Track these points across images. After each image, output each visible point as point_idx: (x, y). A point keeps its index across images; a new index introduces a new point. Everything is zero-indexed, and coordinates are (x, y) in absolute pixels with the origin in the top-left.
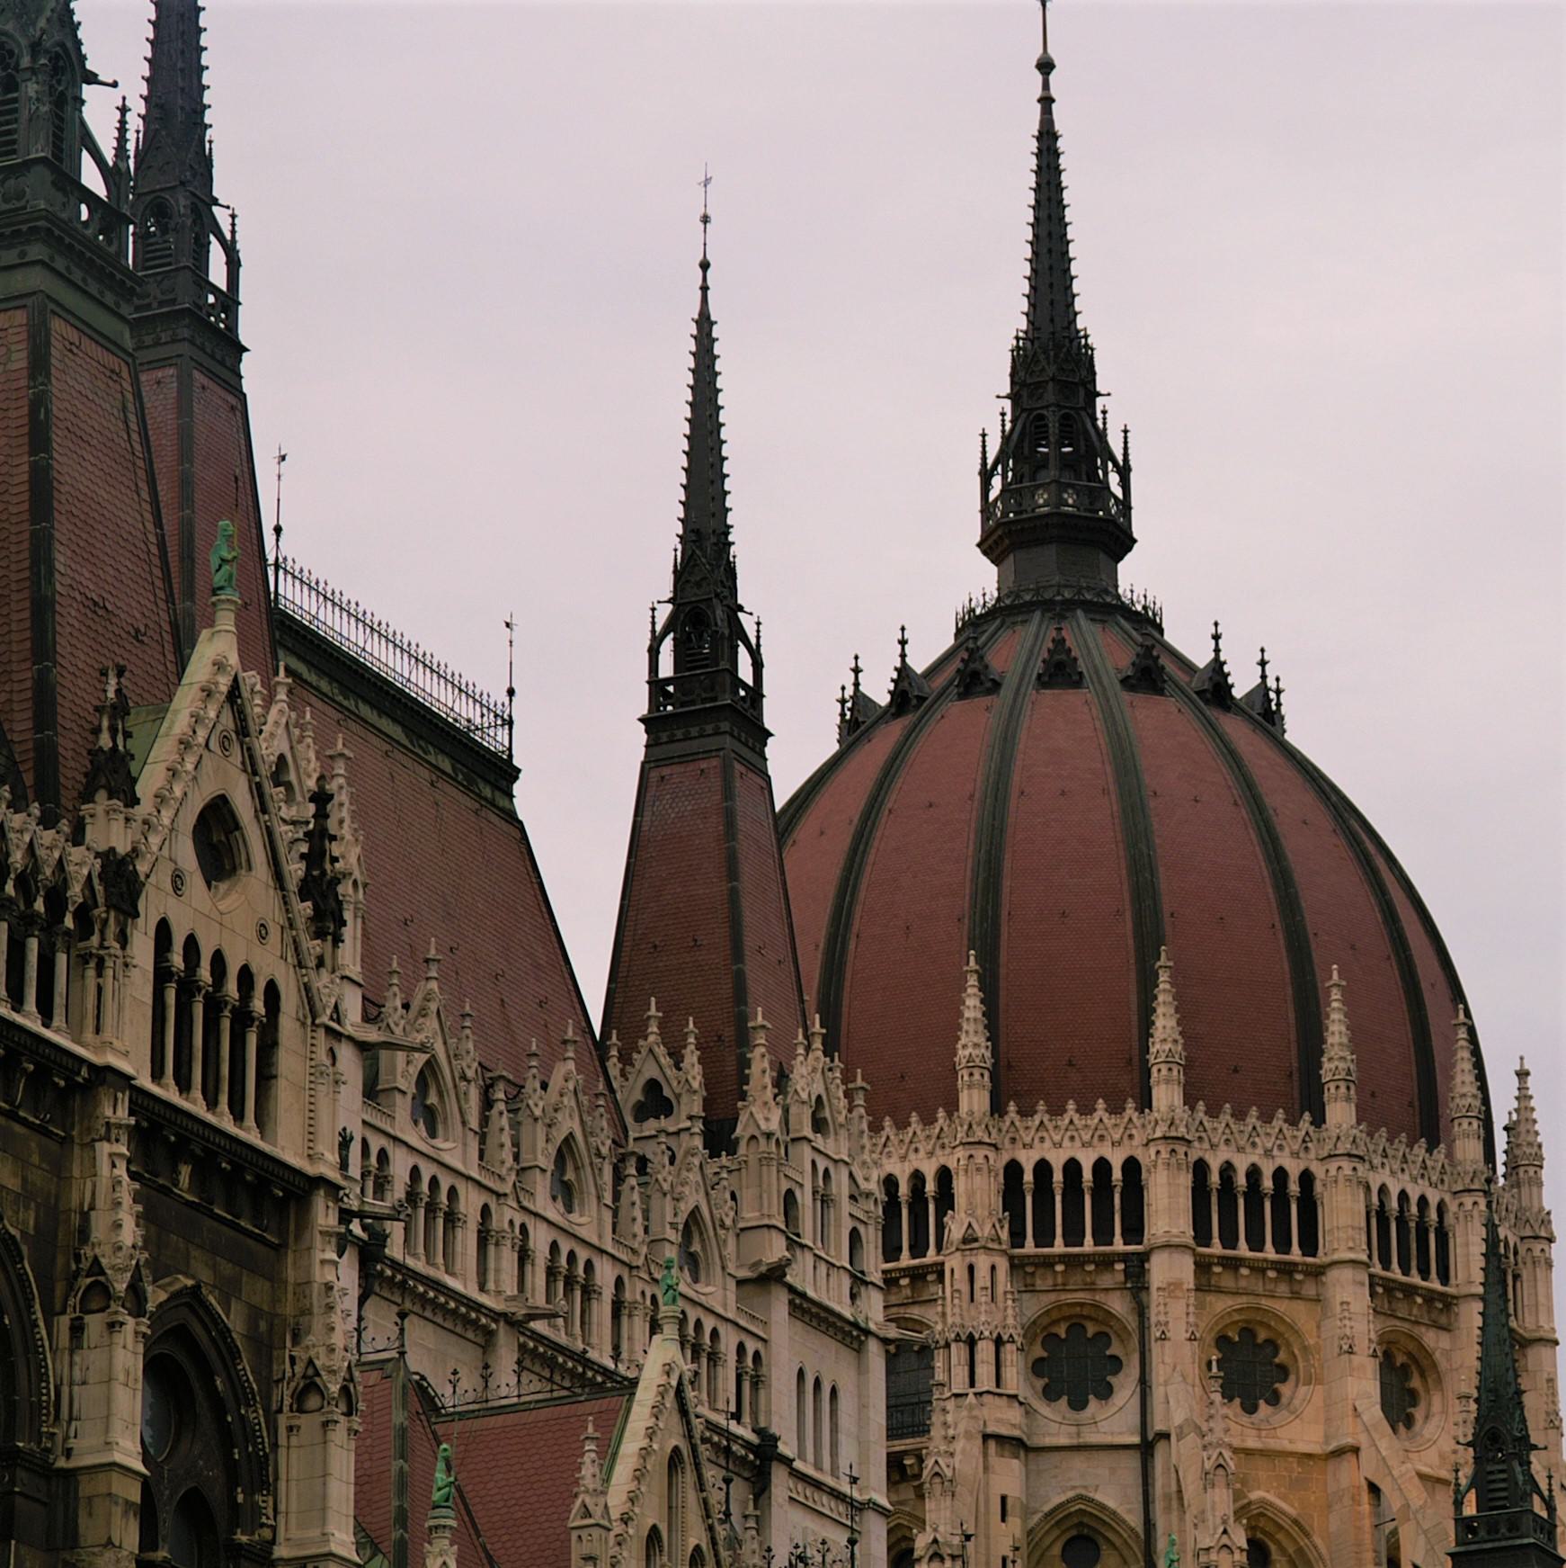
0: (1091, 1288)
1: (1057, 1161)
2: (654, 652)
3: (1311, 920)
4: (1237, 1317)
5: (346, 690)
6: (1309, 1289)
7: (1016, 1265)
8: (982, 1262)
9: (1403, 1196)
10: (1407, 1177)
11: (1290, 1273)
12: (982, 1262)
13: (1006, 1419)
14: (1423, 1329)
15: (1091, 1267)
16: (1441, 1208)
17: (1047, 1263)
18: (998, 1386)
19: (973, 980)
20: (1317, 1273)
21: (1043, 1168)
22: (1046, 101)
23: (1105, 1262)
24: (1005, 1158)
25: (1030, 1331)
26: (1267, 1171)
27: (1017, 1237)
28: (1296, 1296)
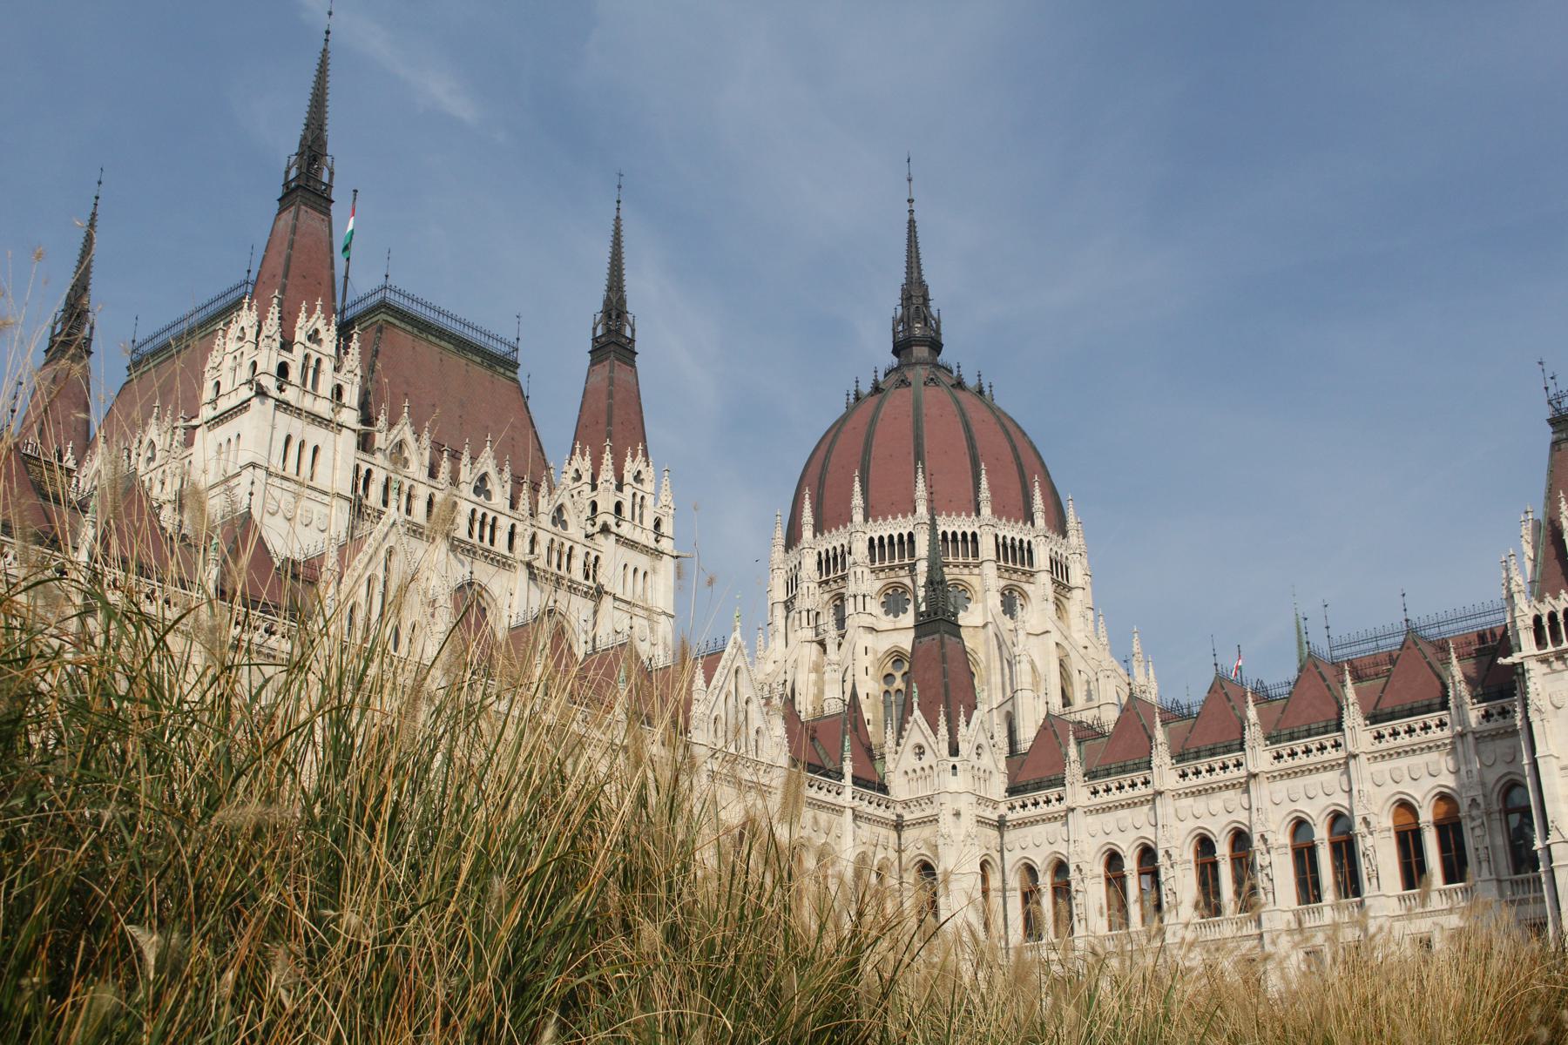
2: (595, 329)
3: (979, 452)
5: (421, 331)
6: (976, 571)
8: (859, 570)
12: (859, 570)
13: (867, 621)
22: (911, 212)
25: (879, 593)
27: (873, 561)
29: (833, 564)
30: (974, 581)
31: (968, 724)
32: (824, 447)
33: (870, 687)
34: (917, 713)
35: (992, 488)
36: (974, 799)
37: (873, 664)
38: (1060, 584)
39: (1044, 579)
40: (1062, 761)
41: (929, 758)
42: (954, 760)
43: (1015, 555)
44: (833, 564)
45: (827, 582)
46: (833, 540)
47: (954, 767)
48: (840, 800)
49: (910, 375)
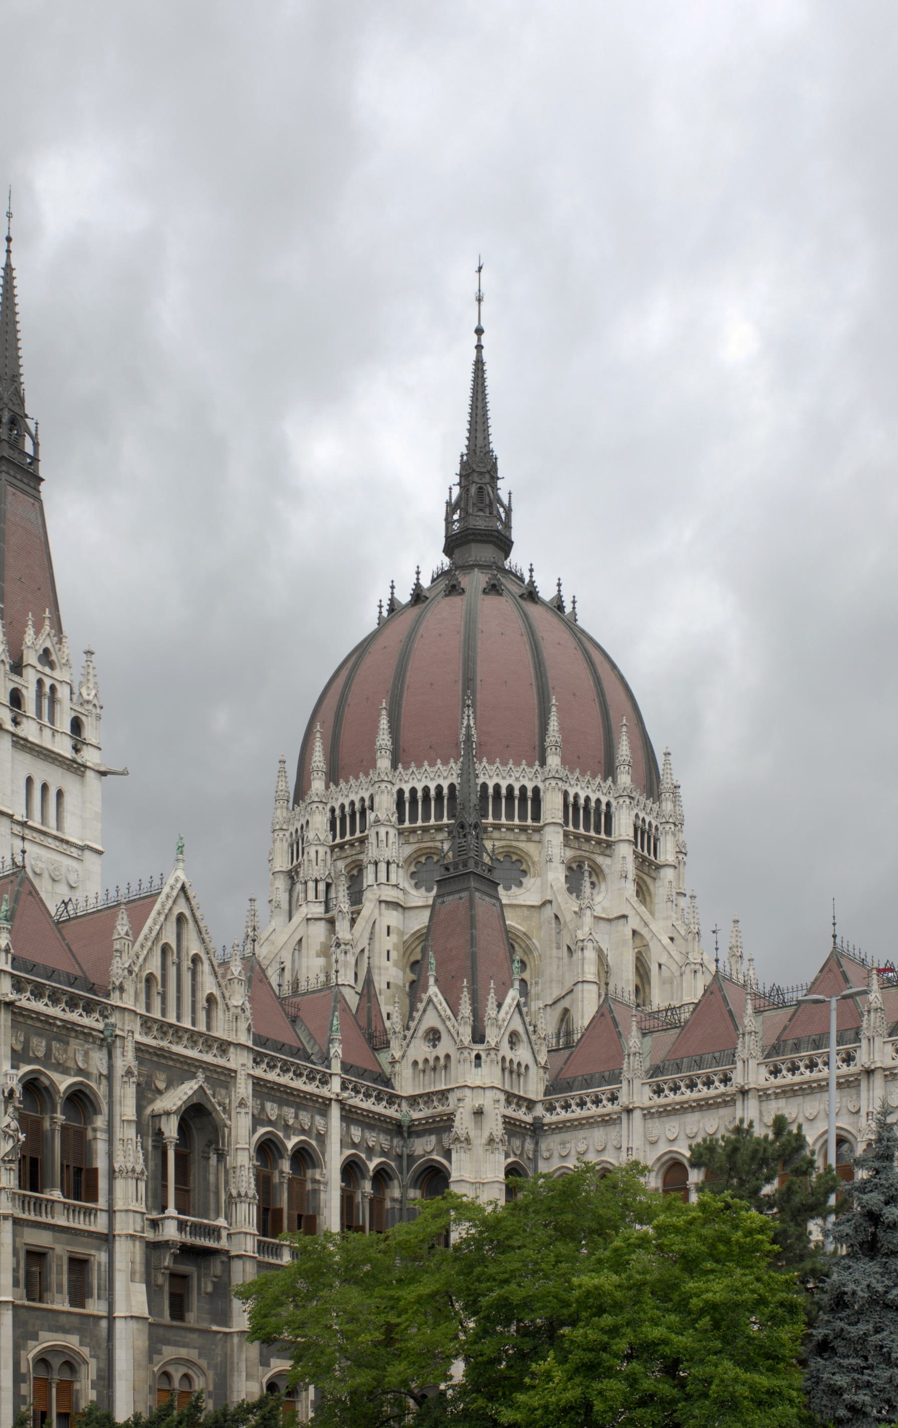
0: (433, 840)
1: (419, 787)
4: (501, 850)
6: (536, 837)
7: (401, 833)
8: (382, 831)
9: (588, 799)
10: (590, 790)
11: (526, 830)
12: (382, 831)
14: (596, 856)
15: (433, 831)
16: (608, 805)
17: (413, 831)
18: (388, 880)
19: (384, 712)
20: (539, 830)
21: (413, 791)
23: (439, 829)
24: (396, 788)
25: (408, 860)
26: (517, 787)
27: (401, 820)
28: (529, 840)
29: (349, 823)
30: (530, 848)
31: (499, 1006)
32: (345, 673)
33: (390, 974)
34: (433, 990)
35: (562, 729)
36: (502, 1097)
37: (396, 947)
38: (644, 859)
39: (625, 851)
40: (619, 1054)
41: (445, 1047)
42: (479, 1048)
43: (589, 821)
44: (349, 823)
45: (341, 846)
46: (350, 794)
47: (478, 1057)
48: (324, 1092)
49: (465, 581)
